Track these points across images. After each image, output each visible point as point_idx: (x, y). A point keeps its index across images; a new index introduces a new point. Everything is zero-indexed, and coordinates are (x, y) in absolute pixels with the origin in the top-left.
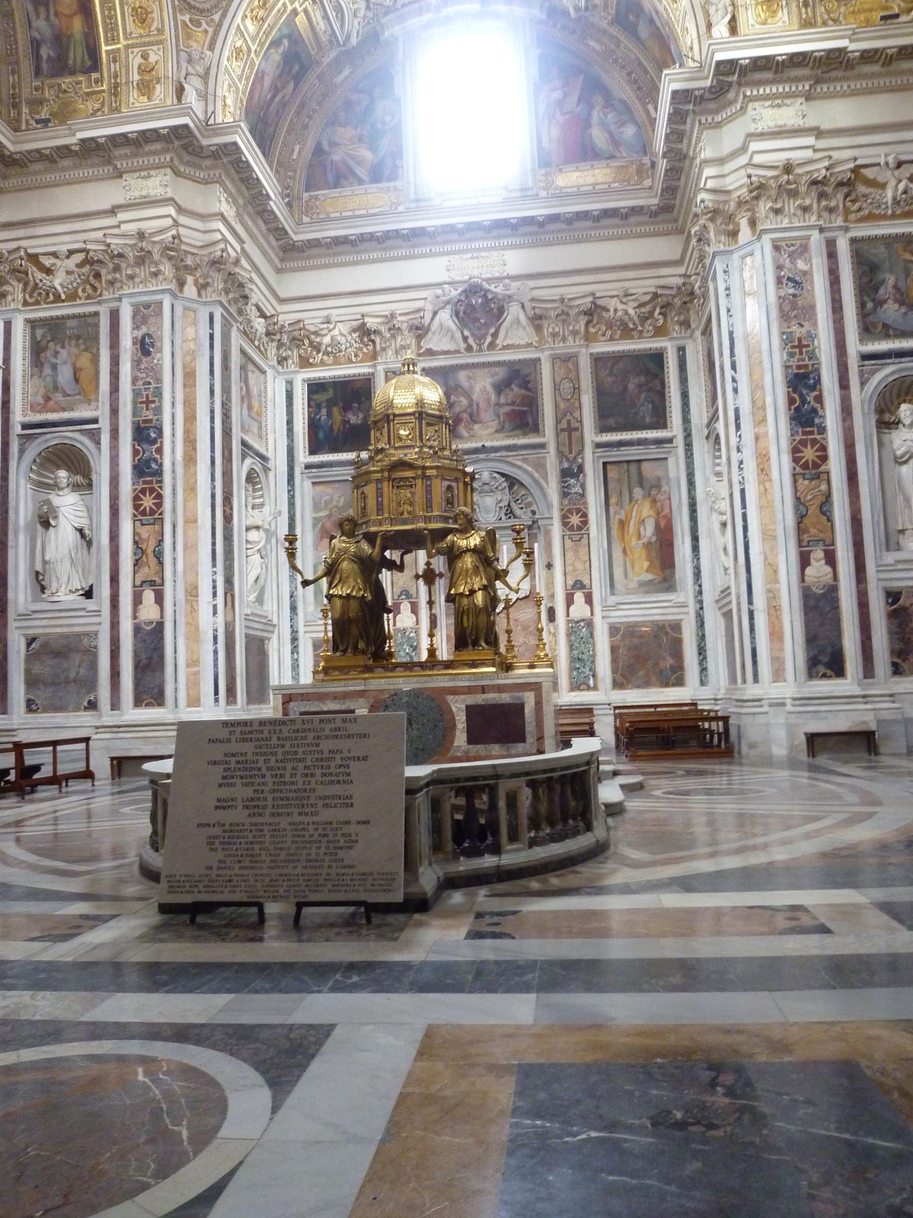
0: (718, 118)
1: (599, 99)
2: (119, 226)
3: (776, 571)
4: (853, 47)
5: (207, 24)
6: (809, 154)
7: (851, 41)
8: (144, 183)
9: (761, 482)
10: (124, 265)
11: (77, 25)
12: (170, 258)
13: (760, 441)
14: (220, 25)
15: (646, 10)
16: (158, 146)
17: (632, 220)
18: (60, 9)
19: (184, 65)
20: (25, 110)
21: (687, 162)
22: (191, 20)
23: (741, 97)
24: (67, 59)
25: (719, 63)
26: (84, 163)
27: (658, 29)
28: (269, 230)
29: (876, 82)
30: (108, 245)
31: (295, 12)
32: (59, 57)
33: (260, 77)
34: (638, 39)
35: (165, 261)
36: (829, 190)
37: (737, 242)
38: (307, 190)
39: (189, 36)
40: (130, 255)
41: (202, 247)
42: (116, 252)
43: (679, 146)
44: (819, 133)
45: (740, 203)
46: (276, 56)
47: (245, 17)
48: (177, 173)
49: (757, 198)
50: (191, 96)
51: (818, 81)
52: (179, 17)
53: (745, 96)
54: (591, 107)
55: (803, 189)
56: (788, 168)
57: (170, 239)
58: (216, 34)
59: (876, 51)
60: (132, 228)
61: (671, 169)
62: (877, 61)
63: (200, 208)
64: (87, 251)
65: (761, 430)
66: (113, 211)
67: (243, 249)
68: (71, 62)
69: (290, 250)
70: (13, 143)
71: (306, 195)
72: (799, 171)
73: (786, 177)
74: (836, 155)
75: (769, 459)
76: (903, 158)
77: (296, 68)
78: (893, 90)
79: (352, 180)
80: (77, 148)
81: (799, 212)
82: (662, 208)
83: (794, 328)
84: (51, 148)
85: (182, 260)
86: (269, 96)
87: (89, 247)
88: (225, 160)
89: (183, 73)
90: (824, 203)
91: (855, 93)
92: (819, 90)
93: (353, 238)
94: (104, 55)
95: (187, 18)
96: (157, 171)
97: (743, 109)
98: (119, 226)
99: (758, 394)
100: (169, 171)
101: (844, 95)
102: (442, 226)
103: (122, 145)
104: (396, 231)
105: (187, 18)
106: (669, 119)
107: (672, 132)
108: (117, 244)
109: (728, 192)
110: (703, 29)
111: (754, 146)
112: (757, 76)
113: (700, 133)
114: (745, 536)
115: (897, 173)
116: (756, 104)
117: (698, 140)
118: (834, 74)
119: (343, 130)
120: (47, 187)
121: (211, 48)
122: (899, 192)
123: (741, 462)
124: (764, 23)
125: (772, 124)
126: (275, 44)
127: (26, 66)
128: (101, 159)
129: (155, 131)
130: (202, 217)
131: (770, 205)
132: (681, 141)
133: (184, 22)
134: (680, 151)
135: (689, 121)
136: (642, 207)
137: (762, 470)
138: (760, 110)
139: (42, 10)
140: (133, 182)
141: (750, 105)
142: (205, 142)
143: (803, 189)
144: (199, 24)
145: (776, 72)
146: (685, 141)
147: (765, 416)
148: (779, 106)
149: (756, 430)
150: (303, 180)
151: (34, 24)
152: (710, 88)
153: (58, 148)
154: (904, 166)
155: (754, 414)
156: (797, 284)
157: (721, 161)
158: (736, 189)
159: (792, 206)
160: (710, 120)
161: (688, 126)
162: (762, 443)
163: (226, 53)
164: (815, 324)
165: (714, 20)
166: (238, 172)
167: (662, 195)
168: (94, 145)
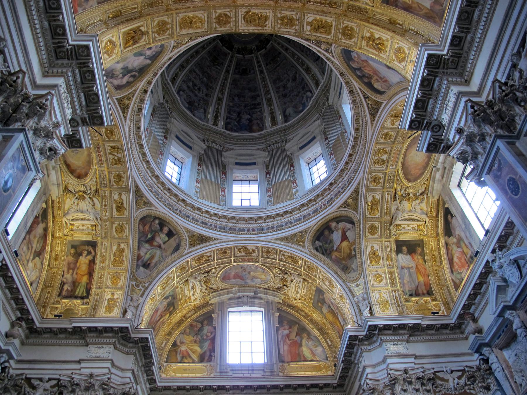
0: (369, 348)
1: (305, 335)
2: (80, 369)
4: (423, 323)
5: (142, 287)
6: (412, 365)
7: (422, 321)
8: (99, 350)
10: (78, 390)
11: (85, 279)
12: (104, 389)
14: (147, 288)
15: (327, 302)
16: (110, 335)
17: (325, 389)
18: (79, 272)
19: (129, 301)
20: (48, 309)
21: (353, 365)
22: (136, 284)
23: (379, 340)
24: (75, 292)
25: (370, 326)
26: (71, 337)
27: (332, 310)
28: (148, 380)
29: (434, 337)
30: (73, 379)
31: (177, 287)
32: (72, 290)
33: (156, 311)
34: (322, 312)
35: (100, 390)
36: (425, 382)
38: (167, 362)
39: (133, 290)
40: (83, 385)
41: (119, 385)
42: (75, 383)
43: (350, 358)
44: (416, 357)
45: (385, 386)
46: (165, 303)
47: (158, 287)
48: (115, 348)
49: (394, 384)
50: (129, 315)
51: (410, 336)
52: (131, 282)
53: (381, 340)
54: (302, 338)
55: (414, 381)
56: (406, 372)
57: (107, 379)
58: (145, 291)
59: (432, 325)
60: (87, 371)
61: (345, 368)
62: (433, 329)
63: (123, 367)
64: (59, 380)
66: (79, 362)
67: (136, 388)
68: (77, 293)
69: (155, 390)
70: (40, 323)
71: (165, 364)
72: (410, 372)
73: (406, 375)
74: (426, 366)
76: (453, 369)
77: (172, 308)
78: (441, 340)
79: (189, 359)
80: (71, 330)
81: (414, 392)
82: (338, 385)
84: (58, 328)
85: (108, 391)
86: (158, 319)
87: (61, 378)
88: (140, 345)
89: (128, 305)
90: (424, 388)
91: (426, 341)
92: (411, 339)
93: (188, 387)
94: (93, 292)
95: (134, 283)
96: (107, 346)
97: (380, 345)
98: (80, 369)
100: (112, 346)
101: (422, 341)
102: (233, 386)
103: (93, 332)
104: (210, 386)
105: (134, 283)
106: (347, 347)
107: (348, 352)
108: (77, 379)
109: (378, 380)
110: (357, 312)
111: (389, 361)
112: (386, 332)
113: (361, 353)
115: (451, 375)
116: (387, 343)
117: (360, 356)
118: (416, 333)
119: (187, 337)
120: (48, 345)
121: (142, 296)
122: (455, 384)
124: (384, 311)
125: (394, 352)
126: (166, 298)
127: (56, 292)
128: (80, 336)
129: (112, 328)
130: (123, 370)
131: (400, 387)
132: (351, 356)
133: (133, 285)
134: (351, 360)
135: (355, 348)
136: (329, 384)
138: (388, 346)
139: (71, 271)
140: (93, 349)
141: (384, 343)
142: (133, 335)
143: (414, 381)
144: (138, 286)
145: (393, 331)
146: (353, 356)
148: (396, 345)
150: (165, 357)
151: (65, 276)
152: (366, 335)
153: (61, 329)
154: (454, 372)
157: (374, 366)
158: (382, 379)
159: (410, 388)
160: (366, 348)
161: (355, 350)
163: (148, 299)
165: (362, 309)
166: (143, 351)
167: (339, 379)
168: (79, 330)
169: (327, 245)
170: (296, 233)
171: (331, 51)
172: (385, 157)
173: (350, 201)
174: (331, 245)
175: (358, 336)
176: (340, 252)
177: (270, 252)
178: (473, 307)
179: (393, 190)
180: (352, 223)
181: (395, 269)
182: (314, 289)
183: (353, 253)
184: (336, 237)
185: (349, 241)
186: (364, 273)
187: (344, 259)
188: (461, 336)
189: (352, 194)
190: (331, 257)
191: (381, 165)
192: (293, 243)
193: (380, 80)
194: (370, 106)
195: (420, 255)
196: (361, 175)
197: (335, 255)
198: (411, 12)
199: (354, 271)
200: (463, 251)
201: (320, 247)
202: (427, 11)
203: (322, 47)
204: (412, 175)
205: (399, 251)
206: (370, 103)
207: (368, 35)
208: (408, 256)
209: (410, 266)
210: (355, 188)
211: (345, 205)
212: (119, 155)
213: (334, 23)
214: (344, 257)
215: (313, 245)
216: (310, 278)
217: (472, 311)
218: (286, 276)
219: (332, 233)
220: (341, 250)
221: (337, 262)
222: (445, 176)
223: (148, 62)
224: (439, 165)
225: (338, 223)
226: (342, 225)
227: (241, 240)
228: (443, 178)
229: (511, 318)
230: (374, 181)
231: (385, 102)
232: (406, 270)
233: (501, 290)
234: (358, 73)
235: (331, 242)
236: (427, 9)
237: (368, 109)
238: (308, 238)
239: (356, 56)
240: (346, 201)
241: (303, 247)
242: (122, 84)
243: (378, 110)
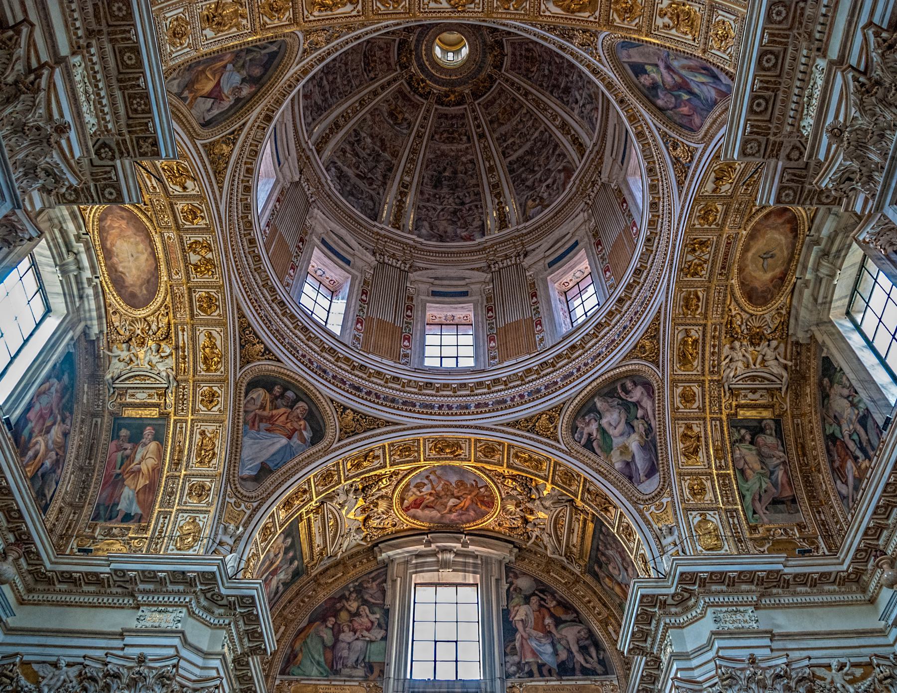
172: (194, 258)
180: (206, 124)
196: (222, 208)
204: (122, 218)
212: (690, 257)
222: (60, 241)
223: (599, 404)
224: (80, 247)
231: (238, 375)
234: (290, 394)
237: (255, 333)
239: (305, 433)
242: (643, 390)
243: (241, 345)
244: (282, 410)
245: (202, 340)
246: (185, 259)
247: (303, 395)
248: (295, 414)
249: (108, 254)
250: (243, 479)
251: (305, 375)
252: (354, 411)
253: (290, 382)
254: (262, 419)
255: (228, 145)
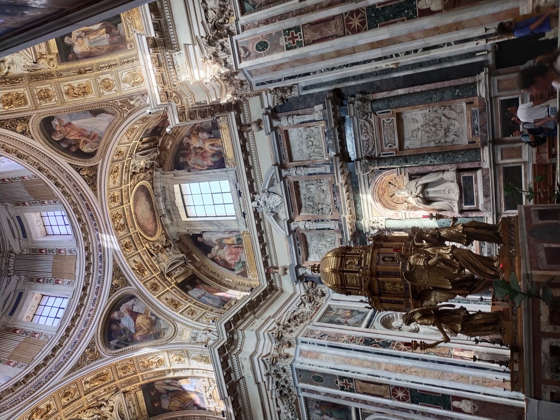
0: (238, 349)
3: (462, 377)
9: (411, 373)
13: (388, 369)
37: (291, 356)
45: (277, 349)
51: (254, 314)
65: (383, 367)
75: (399, 366)
81: (297, 327)
83: (343, 340)
97: (244, 337)
99: (365, 364)
109: (269, 354)
114: (439, 387)
123: (397, 379)
137: (404, 371)
141: (245, 331)
147: (377, 363)
149: (383, 369)
155: (374, 368)
156: (325, 335)
162: (390, 367)
164: (345, 334)
169: (124, 336)
170: (84, 352)
171: (29, 131)
172: (122, 221)
173: (115, 282)
174: (127, 332)
175: (223, 345)
176: (141, 328)
177: (69, 393)
178: (269, 260)
179: (145, 248)
181: (195, 301)
182: (140, 394)
183: (153, 318)
184: (126, 322)
185: (142, 314)
186: (177, 321)
187: (149, 330)
188: (278, 292)
189: (113, 275)
190: (137, 341)
191: (123, 230)
192: (88, 364)
193: (88, 140)
194: (86, 177)
195: (202, 283)
197: (137, 336)
198: (94, 56)
199: (167, 329)
200: (229, 244)
201: (118, 343)
202: (108, 47)
203: (19, 128)
204: (150, 231)
205: (186, 291)
206: (85, 173)
207: (66, 88)
208: (195, 289)
209: (203, 293)
210: (113, 267)
211: (114, 289)
213: (26, 92)
214: (147, 329)
215: (110, 348)
216: (130, 382)
217: (270, 265)
218: (103, 409)
219: (120, 322)
220: (140, 326)
221: (146, 338)
225: (118, 310)
226: (123, 308)
227: (25, 406)
228: (172, 220)
229: (296, 226)
230: (127, 248)
232: (203, 297)
233: (276, 217)
234: (64, 146)
235: (125, 330)
236: (107, 45)
237: (86, 181)
238: (100, 346)
239: (57, 123)
240: (112, 285)
241: (101, 357)
244: (71, 138)
245: (118, 180)
246: (125, 220)
247: (56, 145)
248: (62, 135)
249: (152, 209)
250: (113, 115)
251: (51, 154)
252: (15, 131)
253: (63, 152)
254: (88, 137)
255: (116, 284)
